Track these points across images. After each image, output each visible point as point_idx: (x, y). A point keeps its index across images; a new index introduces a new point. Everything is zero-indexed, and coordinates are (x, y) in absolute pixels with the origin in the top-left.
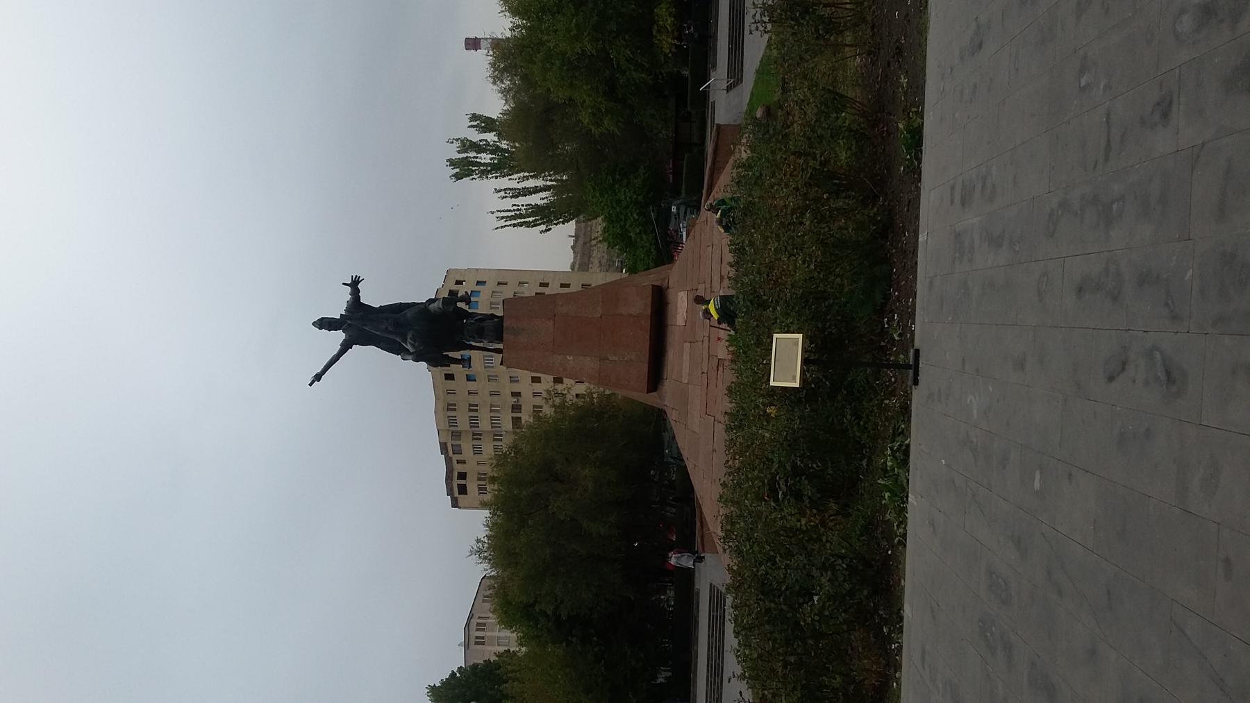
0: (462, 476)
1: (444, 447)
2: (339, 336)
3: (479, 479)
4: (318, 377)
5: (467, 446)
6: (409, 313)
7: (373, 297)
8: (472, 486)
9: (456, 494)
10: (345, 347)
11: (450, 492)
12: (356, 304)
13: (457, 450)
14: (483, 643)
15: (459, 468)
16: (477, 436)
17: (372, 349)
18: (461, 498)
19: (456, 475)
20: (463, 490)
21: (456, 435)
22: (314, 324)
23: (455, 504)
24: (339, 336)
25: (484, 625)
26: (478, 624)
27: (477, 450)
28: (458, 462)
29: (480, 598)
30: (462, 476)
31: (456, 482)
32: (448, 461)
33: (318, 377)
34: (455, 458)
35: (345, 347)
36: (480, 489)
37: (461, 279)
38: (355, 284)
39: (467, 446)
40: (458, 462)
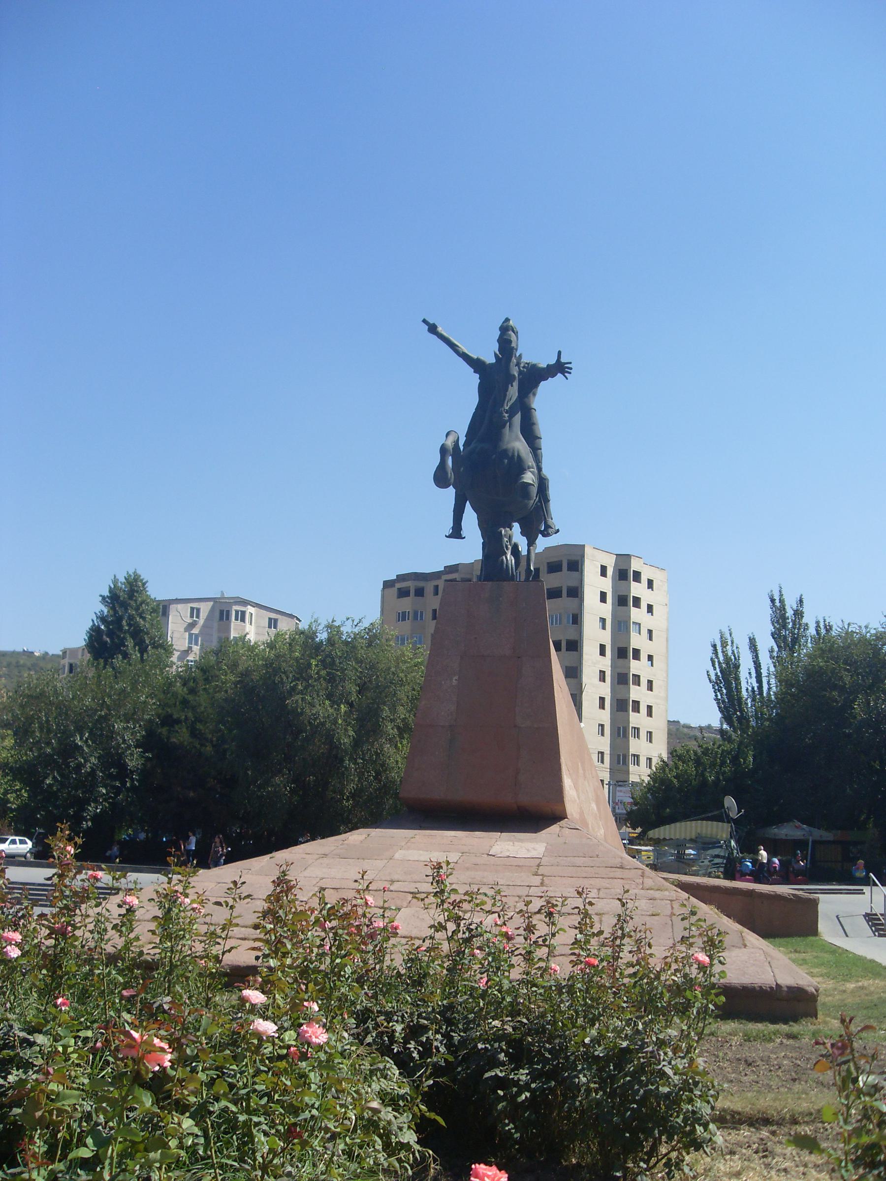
0: (420, 592)
3: (416, 613)
4: (433, 329)
6: (520, 445)
7: (546, 400)
8: (407, 604)
9: (398, 586)
10: (476, 364)
11: (401, 578)
14: (221, 618)
15: (429, 587)
17: (472, 400)
18: (394, 591)
19: (421, 584)
20: (403, 593)
22: (507, 320)
23: (387, 584)
25: (243, 620)
26: (243, 613)
28: (436, 588)
29: (273, 616)
30: (420, 592)
31: (411, 585)
32: (436, 575)
33: (433, 329)
34: (441, 583)
35: (476, 364)
36: (404, 613)
38: (560, 368)
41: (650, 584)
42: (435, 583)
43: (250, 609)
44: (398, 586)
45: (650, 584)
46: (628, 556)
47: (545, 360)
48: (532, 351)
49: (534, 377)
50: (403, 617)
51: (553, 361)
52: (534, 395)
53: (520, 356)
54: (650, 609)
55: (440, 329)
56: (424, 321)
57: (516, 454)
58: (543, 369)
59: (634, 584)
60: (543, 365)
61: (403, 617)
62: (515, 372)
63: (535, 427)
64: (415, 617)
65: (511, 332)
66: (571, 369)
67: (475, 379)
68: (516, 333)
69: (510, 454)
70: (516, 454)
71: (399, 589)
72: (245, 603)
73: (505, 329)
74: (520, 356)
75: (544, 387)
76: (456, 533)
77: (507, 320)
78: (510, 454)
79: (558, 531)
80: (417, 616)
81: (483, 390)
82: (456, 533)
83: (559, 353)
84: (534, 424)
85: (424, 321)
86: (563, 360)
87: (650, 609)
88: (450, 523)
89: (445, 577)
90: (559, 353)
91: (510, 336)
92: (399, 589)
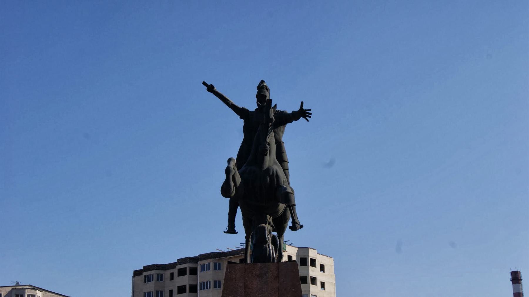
0: (160, 278)
1: (182, 261)
2: (252, 106)
4: (211, 89)
5: (185, 280)
7: (291, 135)
8: (151, 287)
10: (241, 112)
11: (147, 268)
12: (285, 119)
13: (182, 272)
16: (194, 289)
18: (141, 278)
21: (194, 271)
22: (262, 82)
23: (137, 273)
24: (252, 106)
27: (182, 290)
28: (172, 275)
32: (172, 266)
33: (211, 89)
34: (175, 271)
35: (241, 112)
37: (326, 269)
38: (303, 113)
39: (185, 280)
40: (172, 275)
41: (322, 268)
42: (171, 271)
43: (39, 293)
44: (145, 274)
45: (322, 268)
46: (306, 249)
47: (290, 108)
48: (283, 102)
49: (285, 119)
51: (297, 108)
52: (283, 132)
53: (276, 105)
54: (323, 285)
55: (216, 89)
56: (204, 83)
58: (289, 114)
59: (311, 268)
60: (289, 111)
62: (272, 116)
63: (284, 155)
65: (265, 90)
66: (311, 114)
67: (241, 123)
69: (271, 174)
71: (145, 276)
72: (35, 288)
73: (262, 89)
74: (276, 105)
75: (290, 128)
76: (231, 230)
77: (262, 82)
78: (271, 174)
79: (302, 227)
81: (246, 129)
82: (231, 230)
83: (302, 103)
84: (283, 152)
85: (204, 83)
86: (305, 108)
87: (323, 285)
88: (227, 224)
89: (178, 267)
90: (302, 103)
91: (265, 92)
92: (145, 276)
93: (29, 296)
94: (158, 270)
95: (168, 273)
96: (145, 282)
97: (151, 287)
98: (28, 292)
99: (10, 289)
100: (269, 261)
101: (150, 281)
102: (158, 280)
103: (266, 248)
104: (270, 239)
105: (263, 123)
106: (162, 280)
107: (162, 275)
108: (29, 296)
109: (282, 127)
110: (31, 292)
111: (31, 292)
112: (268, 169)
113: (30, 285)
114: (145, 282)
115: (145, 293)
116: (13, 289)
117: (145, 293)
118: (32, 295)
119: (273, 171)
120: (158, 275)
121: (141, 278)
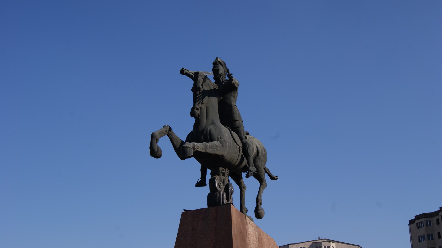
0: (429, 224)
3: (428, 235)
4: (182, 72)
8: (422, 231)
11: (417, 217)
18: (415, 225)
20: (419, 226)
22: (217, 58)
23: (411, 222)
28: (438, 220)
32: (436, 213)
34: (439, 217)
40: (438, 220)
42: (437, 217)
43: (332, 245)
44: (417, 222)
50: (421, 239)
57: (208, 132)
61: (421, 239)
64: (429, 239)
68: (224, 65)
69: (205, 133)
70: (208, 132)
71: (417, 224)
73: (216, 64)
77: (217, 58)
78: (205, 133)
80: (430, 237)
84: (233, 113)
91: (218, 67)
93: (325, 247)
94: (427, 217)
95: (434, 219)
96: (418, 228)
97: (422, 231)
98: (324, 244)
99: (311, 243)
100: (220, 205)
101: (422, 227)
102: (427, 225)
103: (217, 195)
104: (223, 187)
105: (218, 93)
106: (430, 225)
107: (430, 222)
108: (325, 247)
109: (232, 92)
110: (326, 244)
111: (326, 244)
112: (203, 130)
113: (325, 239)
114: (418, 228)
115: (419, 237)
116: (313, 243)
117: (419, 237)
118: (327, 246)
119: (207, 131)
120: (427, 221)
121: (415, 225)
